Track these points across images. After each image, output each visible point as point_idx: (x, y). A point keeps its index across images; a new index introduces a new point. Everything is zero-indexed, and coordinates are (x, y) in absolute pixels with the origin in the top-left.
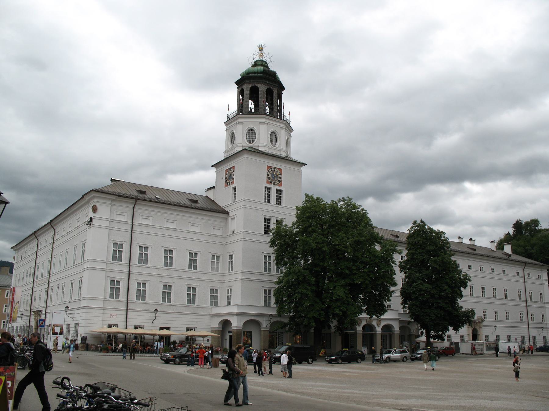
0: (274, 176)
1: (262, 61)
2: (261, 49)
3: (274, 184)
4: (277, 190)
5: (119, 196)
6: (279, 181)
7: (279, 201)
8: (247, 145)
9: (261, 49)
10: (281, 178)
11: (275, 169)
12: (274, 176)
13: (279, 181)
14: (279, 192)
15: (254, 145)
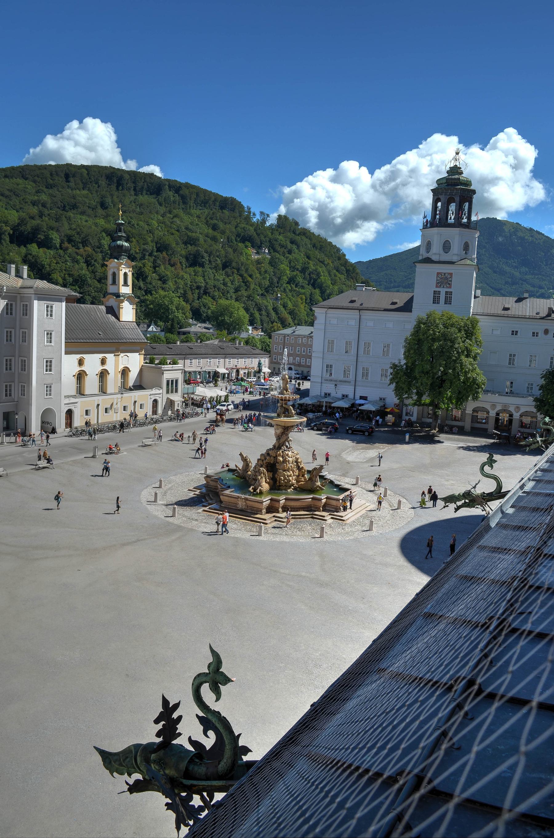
0: (444, 280)
1: (456, 165)
2: (457, 153)
3: (443, 287)
4: (446, 292)
5: (330, 308)
6: (449, 284)
7: (448, 301)
8: (426, 255)
9: (457, 153)
10: (451, 281)
11: (445, 274)
12: (444, 280)
13: (449, 284)
14: (449, 295)
15: (429, 255)
